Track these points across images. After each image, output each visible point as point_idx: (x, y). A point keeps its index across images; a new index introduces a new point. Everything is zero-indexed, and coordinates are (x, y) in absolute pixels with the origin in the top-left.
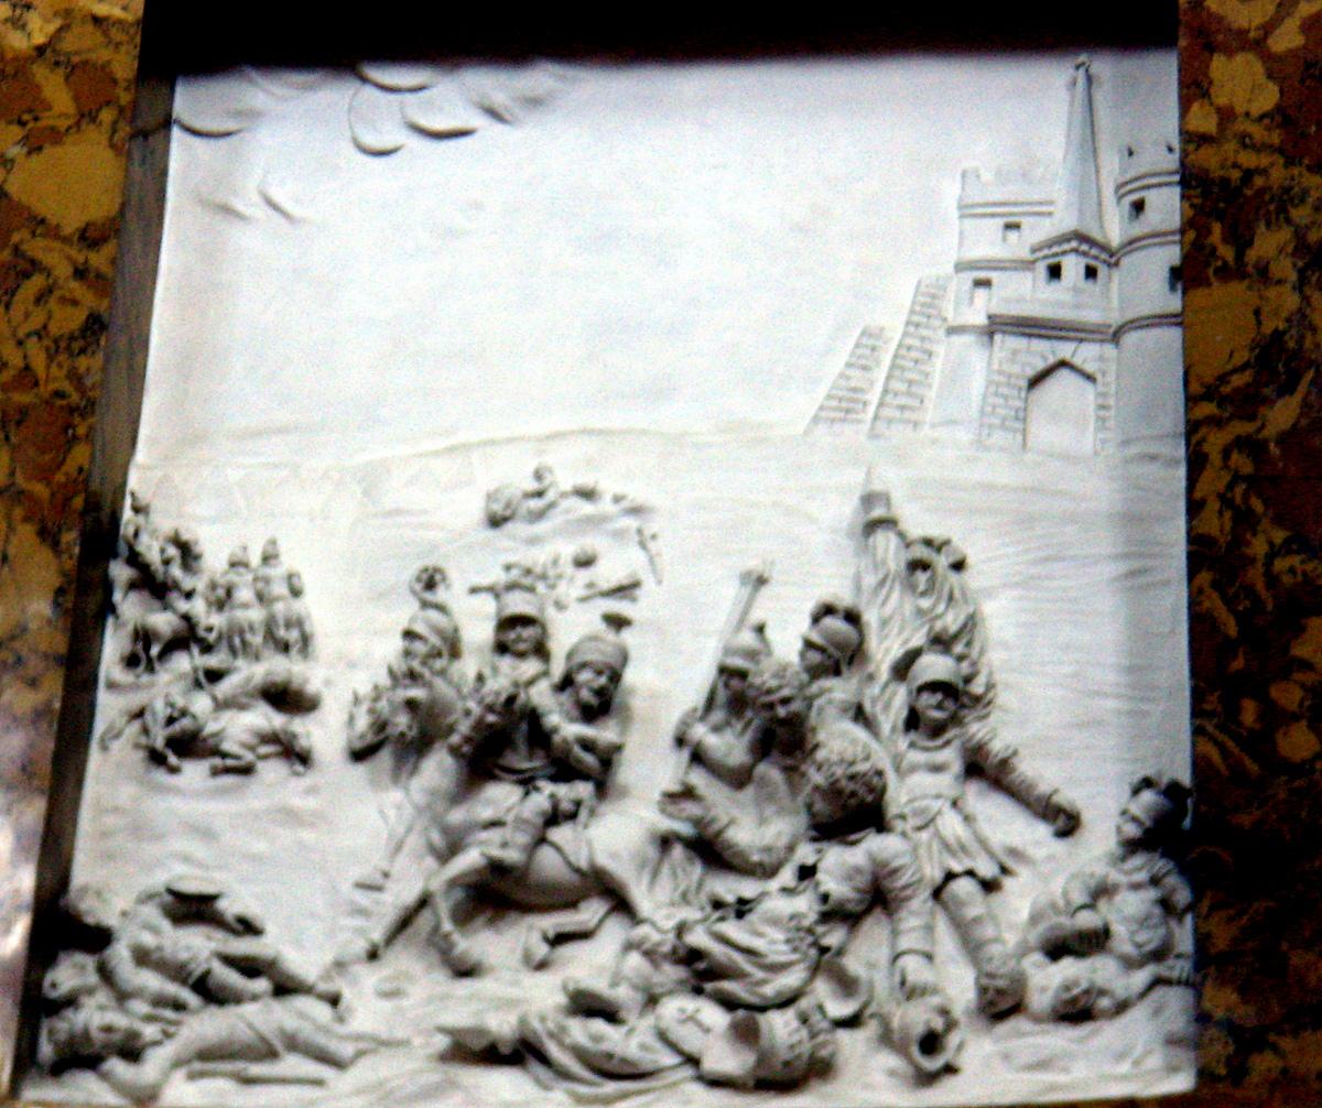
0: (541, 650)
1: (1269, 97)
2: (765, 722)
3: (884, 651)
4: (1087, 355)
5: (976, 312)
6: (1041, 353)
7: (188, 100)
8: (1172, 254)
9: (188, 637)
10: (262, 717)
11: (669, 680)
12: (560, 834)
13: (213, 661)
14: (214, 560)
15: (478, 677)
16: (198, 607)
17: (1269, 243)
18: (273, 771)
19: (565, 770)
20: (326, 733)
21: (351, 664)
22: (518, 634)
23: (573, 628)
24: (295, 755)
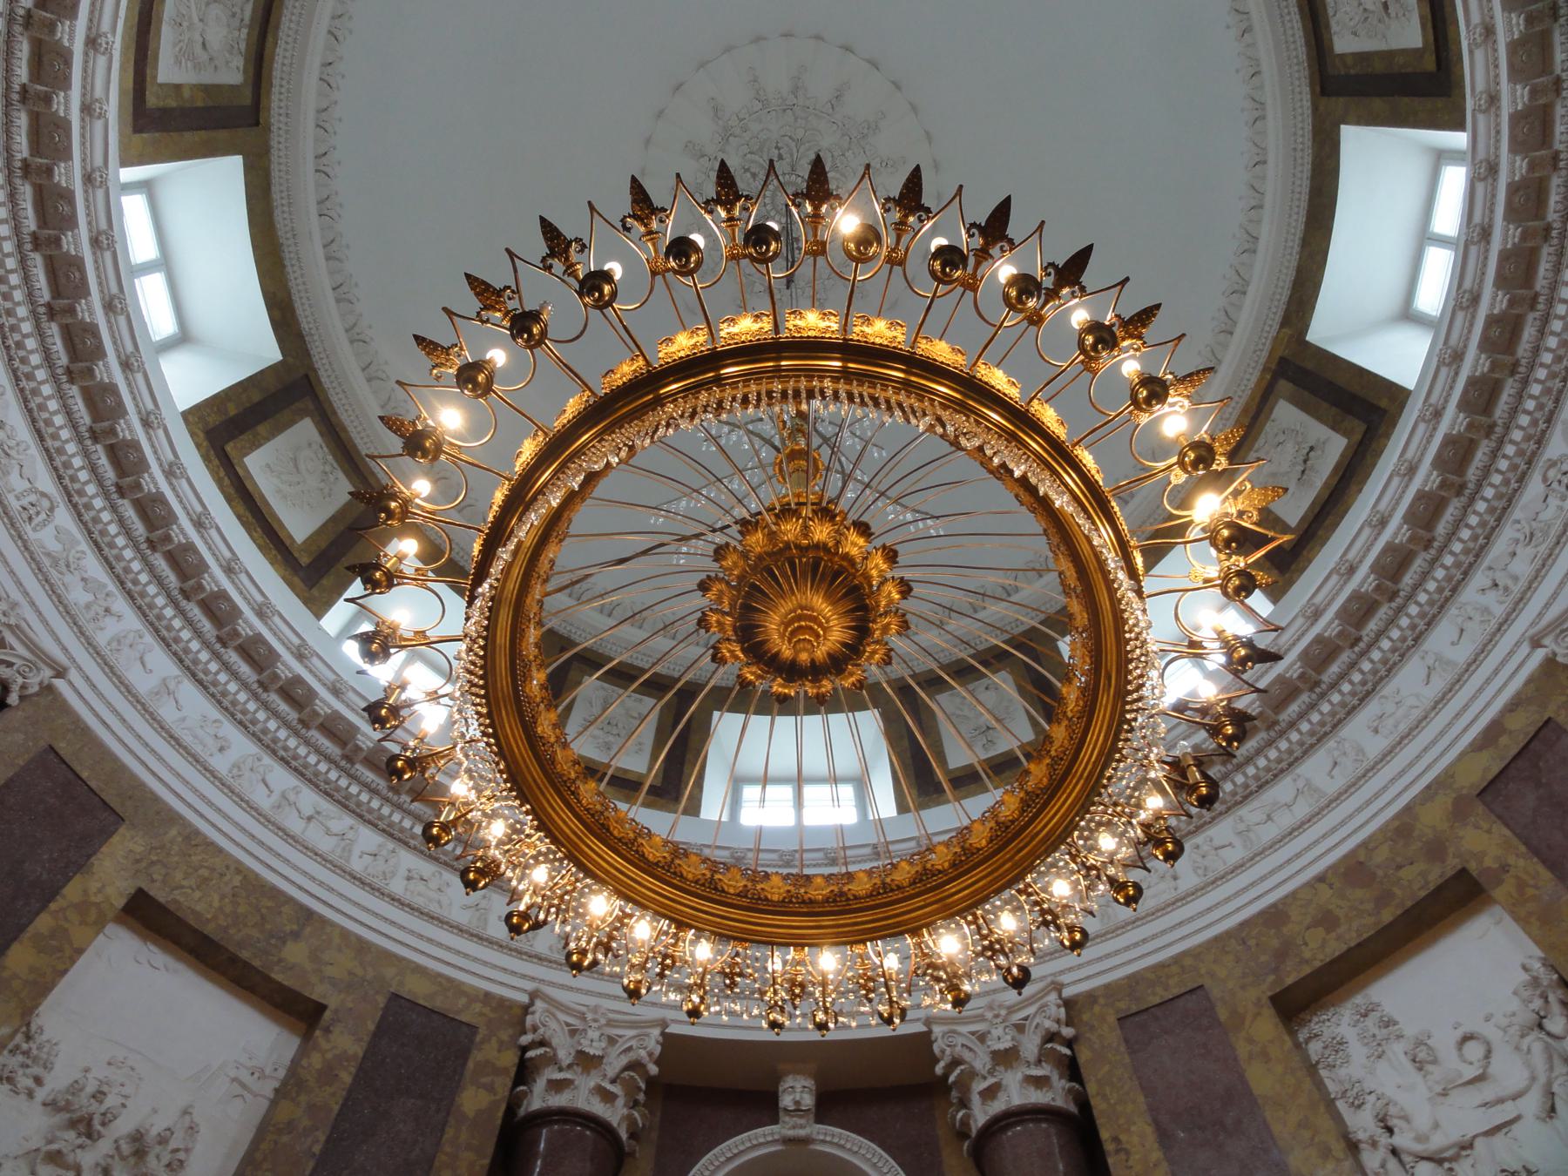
0: (101, 1102)
1: (318, 1066)
2: (139, 1146)
3: (173, 1145)
4: (248, 1096)
5: (233, 1074)
6: (239, 1090)
7: (112, 929)
8: (277, 1084)
9: (26, 1053)
10: (30, 1083)
11: (123, 1126)
12: (78, 1151)
13: (29, 1062)
14: (44, 1038)
15: (84, 1104)
16: (34, 1046)
17: (303, 1098)
18: (23, 1097)
19: (89, 1136)
20: (41, 1094)
21: (57, 1081)
22: (99, 1096)
23: (111, 1101)
24: (30, 1094)
